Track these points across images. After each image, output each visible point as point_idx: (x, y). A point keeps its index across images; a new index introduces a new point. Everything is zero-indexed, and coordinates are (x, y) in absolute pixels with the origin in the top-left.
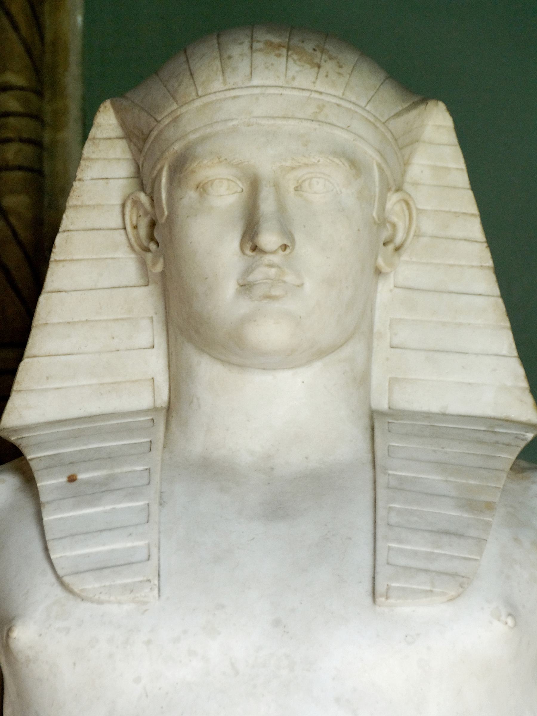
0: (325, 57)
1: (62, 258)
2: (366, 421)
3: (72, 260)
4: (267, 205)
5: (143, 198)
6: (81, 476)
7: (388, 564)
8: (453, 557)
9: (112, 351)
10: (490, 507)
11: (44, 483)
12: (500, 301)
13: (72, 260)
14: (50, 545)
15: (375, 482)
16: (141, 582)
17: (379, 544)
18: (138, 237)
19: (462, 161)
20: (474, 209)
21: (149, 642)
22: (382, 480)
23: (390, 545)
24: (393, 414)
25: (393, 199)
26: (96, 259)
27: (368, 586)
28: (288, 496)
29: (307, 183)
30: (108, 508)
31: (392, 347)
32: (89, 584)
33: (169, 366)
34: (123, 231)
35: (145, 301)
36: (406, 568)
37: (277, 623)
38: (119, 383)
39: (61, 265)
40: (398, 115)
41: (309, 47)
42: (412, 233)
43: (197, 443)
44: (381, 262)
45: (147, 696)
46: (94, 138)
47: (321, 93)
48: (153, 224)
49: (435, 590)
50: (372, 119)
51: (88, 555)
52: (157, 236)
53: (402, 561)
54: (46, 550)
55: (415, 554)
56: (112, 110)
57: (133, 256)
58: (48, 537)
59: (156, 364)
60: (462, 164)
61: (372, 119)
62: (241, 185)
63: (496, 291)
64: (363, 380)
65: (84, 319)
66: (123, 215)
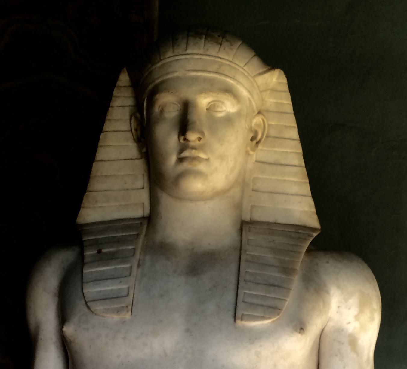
2: (238, 226)
6: (103, 251)
7: (243, 302)
15: (240, 258)
20: (295, 124)
22: (243, 258)
23: (245, 291)
30: (113, 267)
32: (98, 307)
39: (102, 148)
45: (123, 365)
49: (265, 316)
51: (100, 291)
55: (257, 296)
58: (84, 281)
60: (290, 102)
66: (131, 124)
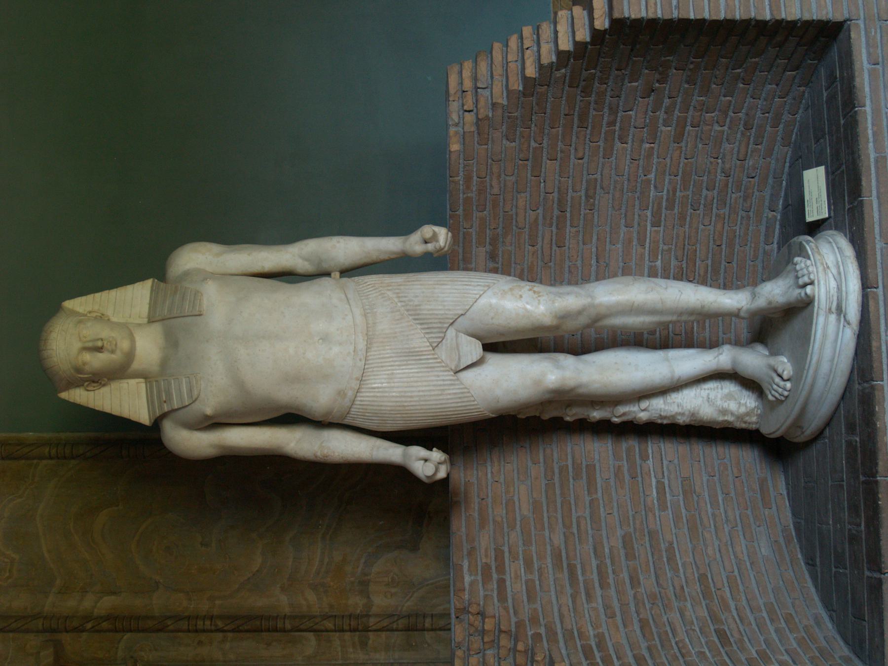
4: (90, 345)
27: (198, 318)
28: (172, 341)
43: (155, 368)
59: (133, 382)
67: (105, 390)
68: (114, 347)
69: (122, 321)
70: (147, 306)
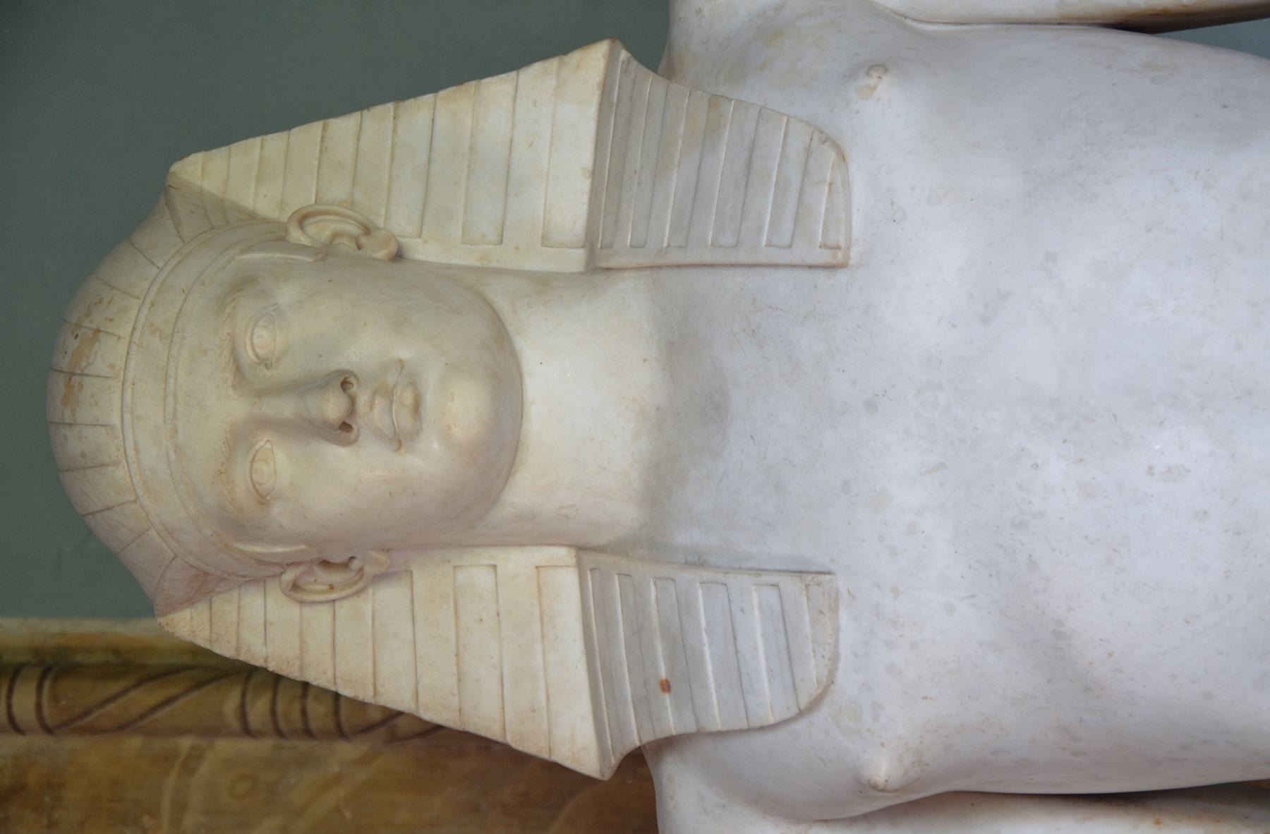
0: (86, 323)
1: (371, 688)
3: (375, 674)
5: (289, 576)
6: (663, 675)
7: (790, 247)
8: (783, 155)
9: (499, 623)
10: (715, 102)
11: (672, 725)
12: (441, 93)
13: (375, 674)
14: (756, 723)
15: (679, 266)
16: (808, 599)
17: (762, 259)
18: (347, 585)
19: (251, 141)
21: (895, 591)
22: (675, 257)
23: (764, 243)
24: (591, 243)
25: (296, 235)
26: (374, 640)
27: (821, 276)
29: (259, 351)
30: (705, 639)
31: (501, 243)
33: (521, 545)
34: (337, 604)
35: (428, 578)
36: (796, 222)
37: (871, 406)
38: (541, 614)
39: (380, 689)
40: (177, 225)
41: (73, 344)
42: (348, 212)
44: (381, 254)
45: (973, 596)
46: (210, 641)
47: (134, 329)
48: (326, 564)
50: (177, 259)
51: (770, 671)
52: (336, 561)
53: (787, 226)
54: (762, 729)
55: (777, 206)
56: (171, 616)
57: (370, 591)
58: (744, 725)
61: (177, 259)
62: (262, 443)
63: (428, 98)
64: (543, 283)
65: (454, 660)
66: (313, 603)
67: (389, 597)
68: (405, 421)
69: (462, 257)
70: (585, 185)
